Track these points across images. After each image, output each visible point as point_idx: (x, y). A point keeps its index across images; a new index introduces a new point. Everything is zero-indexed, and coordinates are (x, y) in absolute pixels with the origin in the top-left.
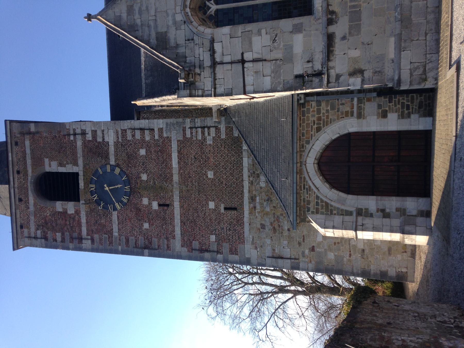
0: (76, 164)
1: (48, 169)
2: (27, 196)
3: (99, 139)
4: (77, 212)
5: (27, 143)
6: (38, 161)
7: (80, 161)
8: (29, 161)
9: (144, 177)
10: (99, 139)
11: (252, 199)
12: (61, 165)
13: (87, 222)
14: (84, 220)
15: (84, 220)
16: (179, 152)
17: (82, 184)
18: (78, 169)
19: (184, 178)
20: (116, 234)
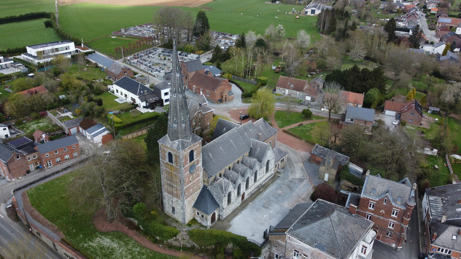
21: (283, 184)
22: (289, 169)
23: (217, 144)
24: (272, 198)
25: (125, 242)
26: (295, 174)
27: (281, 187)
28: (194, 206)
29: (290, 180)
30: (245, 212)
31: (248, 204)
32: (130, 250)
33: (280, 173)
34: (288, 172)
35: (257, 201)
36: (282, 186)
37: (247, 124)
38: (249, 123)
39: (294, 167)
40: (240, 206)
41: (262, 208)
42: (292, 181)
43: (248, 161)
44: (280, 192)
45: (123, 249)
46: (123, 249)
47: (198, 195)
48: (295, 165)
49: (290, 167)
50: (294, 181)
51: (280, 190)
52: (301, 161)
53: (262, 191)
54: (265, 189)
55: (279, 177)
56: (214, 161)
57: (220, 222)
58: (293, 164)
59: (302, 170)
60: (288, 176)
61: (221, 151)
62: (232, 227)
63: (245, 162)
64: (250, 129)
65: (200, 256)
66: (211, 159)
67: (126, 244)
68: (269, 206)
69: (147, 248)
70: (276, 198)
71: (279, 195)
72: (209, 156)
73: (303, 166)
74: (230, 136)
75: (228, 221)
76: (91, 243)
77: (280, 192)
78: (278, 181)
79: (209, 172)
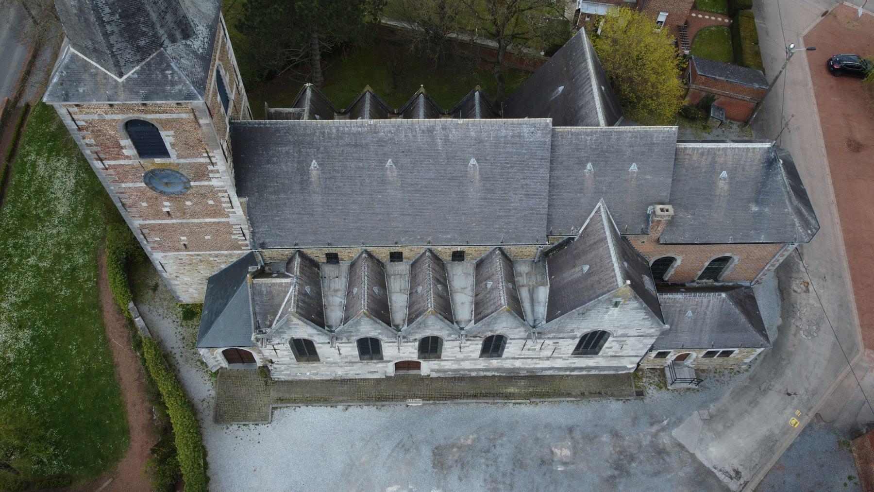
0: (179, 157)
1: (163, 134)
2: (120, 112)
3: (211, 175)
4: (128, 157)
5: (184, 116)
6: (168, 124)
7: (182, 161)
8: (164, 116)
9: (188, 203)
10: (211, 175)
11: (198, 255)
12: (172, 145)
13: (123, 165)
14: (122, 162)
15: (122, 162)
16: (219, 223)
17: (158, 161)
18: (173, 159)
19: (199, 225)
20: (123, 185)
21: (615, 435)
22: (726, 397)
23: (381, 143)
24: (504, 452)
25: (86, 217)
26: (718, 435)
27: (590, 439)
28: (212, 280)
29: (665, 440)
30: (364, 417)
31: (405, 398)
32: (69, 247)
33: (662, 384)
34: (703, 405)
35: (447, 411)
36: (605, 438)
37: (635, 135)
38: (650, 135)
39: (754, 403)
40: (378, 381)
41: (426, 452)
42: (660, 452)
43: (490, 284)
44: (563, 452)
45: (63, 230)
46: (63, 230)
47: (235, 260)
48: (772, 400)
49: (738, 394)
50: (673, 461)
51: (574, 449)
52: (817, 406)
53: (508, 396)
54: (528, 396)
55: (640, 394)
56: (317, 199)
57: (260, 382)
58: (764, 392)
59: (768, 444)
60: (679, 421)
61: (383, 181)
62: (261, 428)
63: (485, 272)
64: (632, 160)
65: (151, 412)
66: (305, 183)
67: (82, 226)
68: (456, 472)
69: (97, 276)
70: (518, 463)
71: (545, 463)
72: (303, 171)
73: (793, 437)
74: (480, 142)
75: (281, 400)
76: (41, 162)
77: (563, 452)
78: (614, 407)
79: (263, 228)
